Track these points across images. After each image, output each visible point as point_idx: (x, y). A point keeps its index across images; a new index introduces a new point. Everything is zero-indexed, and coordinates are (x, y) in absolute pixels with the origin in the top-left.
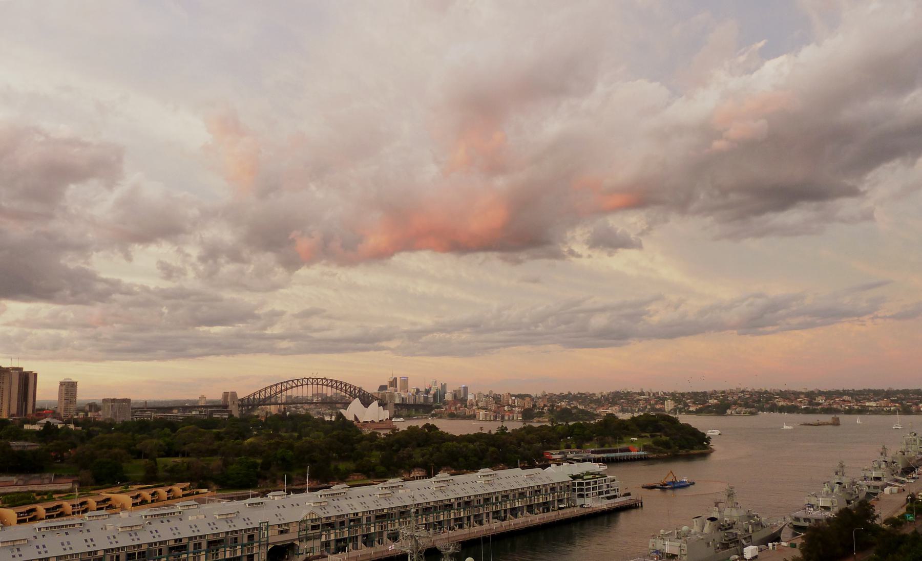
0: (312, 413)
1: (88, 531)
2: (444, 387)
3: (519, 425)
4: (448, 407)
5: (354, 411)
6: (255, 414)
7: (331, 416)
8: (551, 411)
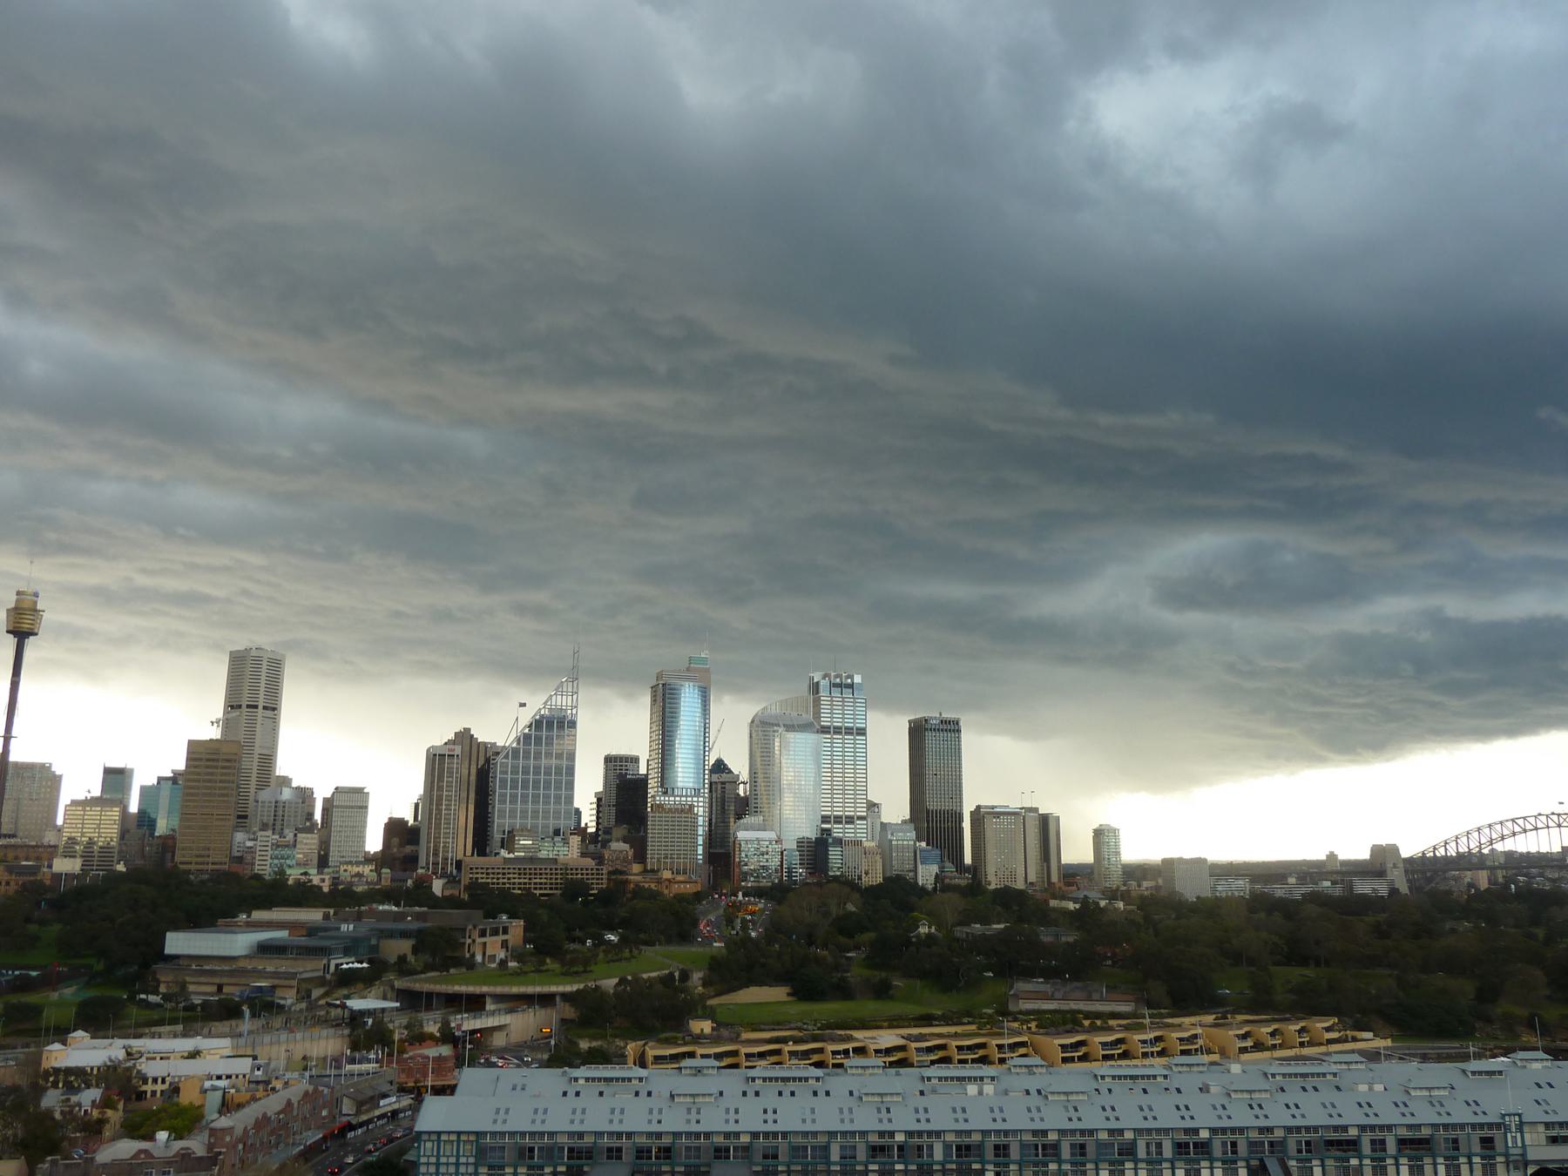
1: (1179, 1091)
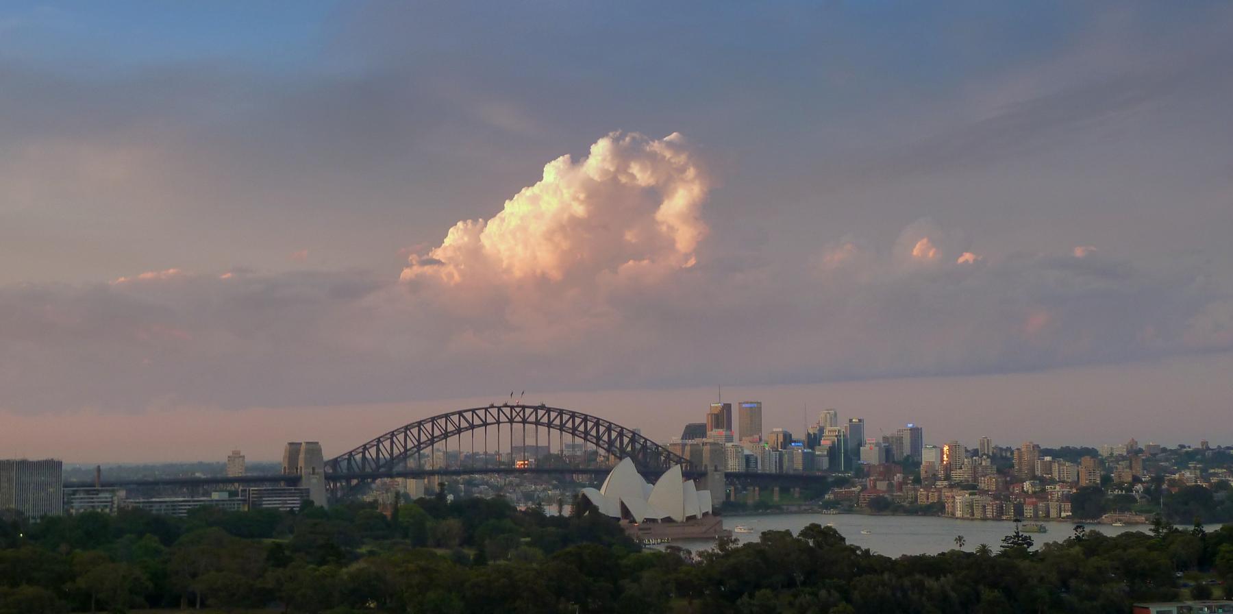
0: (511, 496)
2: (857, 429)
3: (1060, 532)
4: (868, 482)
5: (618, 491)
6: (368, 498)
7: (561, 504)
8: (1153, 494)
